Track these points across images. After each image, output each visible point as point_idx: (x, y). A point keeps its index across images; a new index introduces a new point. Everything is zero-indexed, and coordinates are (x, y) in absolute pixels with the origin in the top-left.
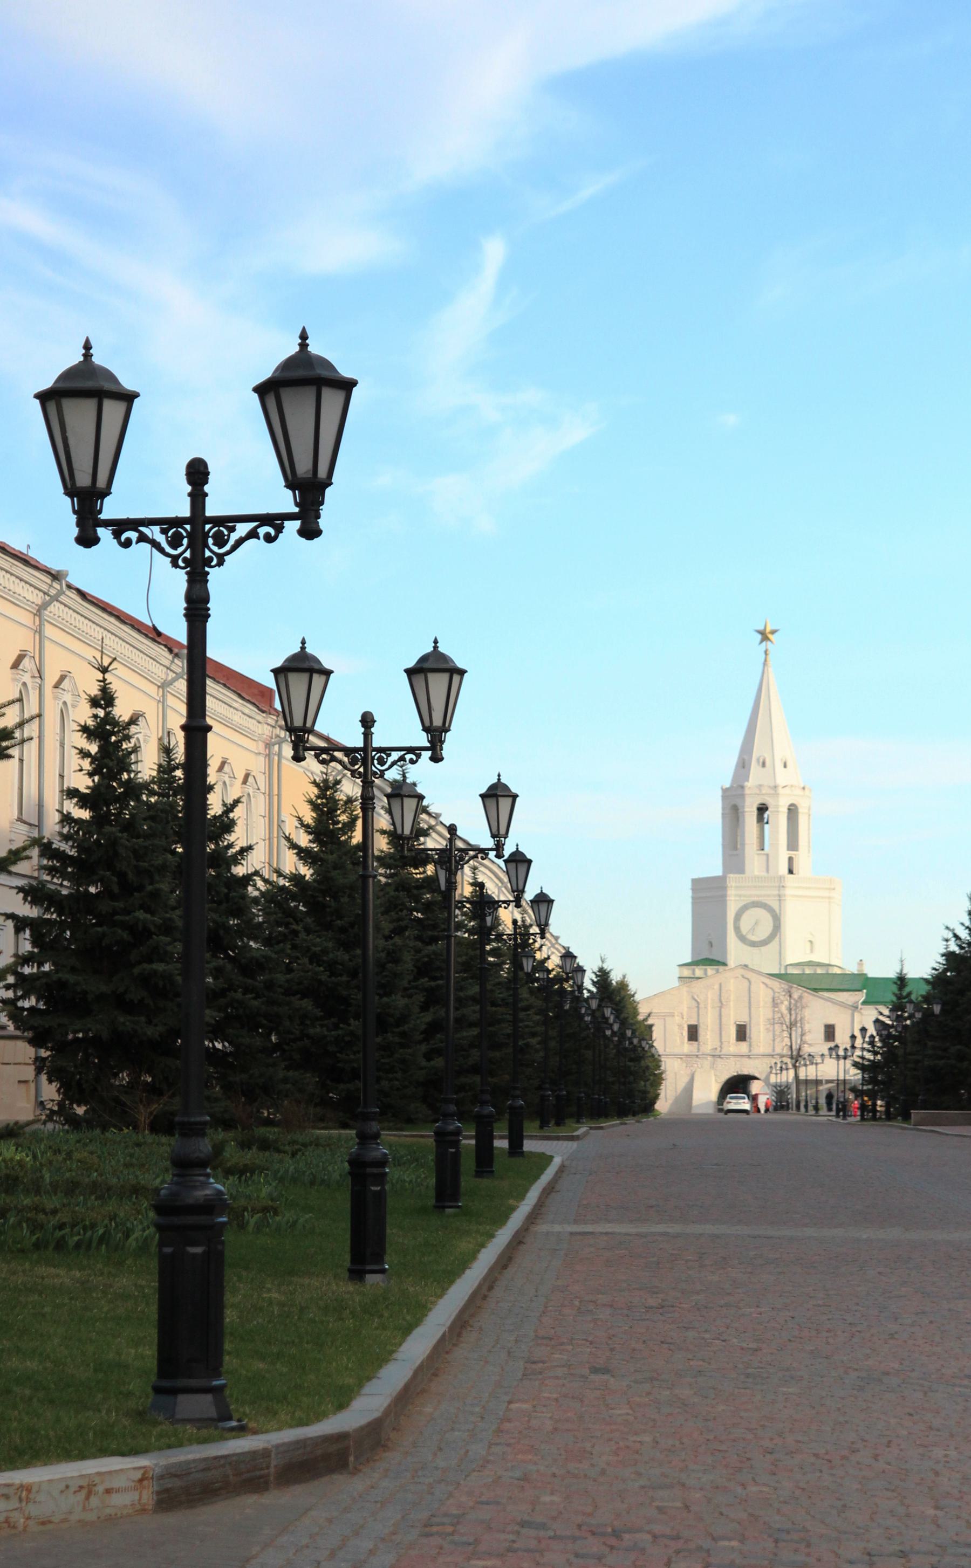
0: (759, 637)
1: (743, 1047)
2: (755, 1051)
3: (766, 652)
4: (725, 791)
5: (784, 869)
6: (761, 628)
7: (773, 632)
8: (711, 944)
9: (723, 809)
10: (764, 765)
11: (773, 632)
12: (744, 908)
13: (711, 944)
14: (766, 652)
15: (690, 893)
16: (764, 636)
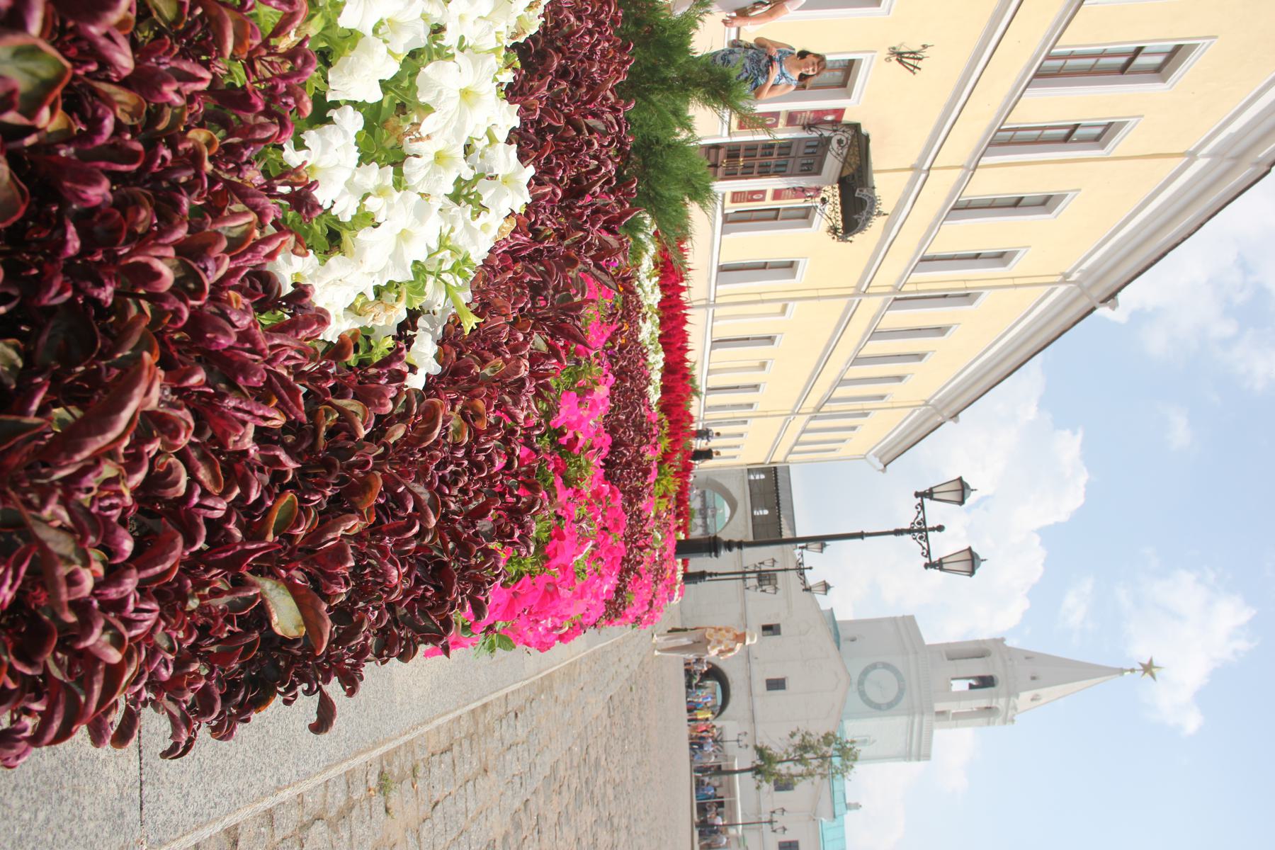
0: (1146, 662)
1: (760, 687)
2: (758, 703)
3: (1132, 670)
4: (1003, 640)
5: (939, 707)
6: (1155, 664)
7: (1153, 675)
8: (853, 640)
9: (984, 641)
10: (1033, 678)
11: (1153, 675)
12: (895, 671)
13: (853, 640)
14: (1132, 670)
15: (900, 615)
16: (1148, 668)
